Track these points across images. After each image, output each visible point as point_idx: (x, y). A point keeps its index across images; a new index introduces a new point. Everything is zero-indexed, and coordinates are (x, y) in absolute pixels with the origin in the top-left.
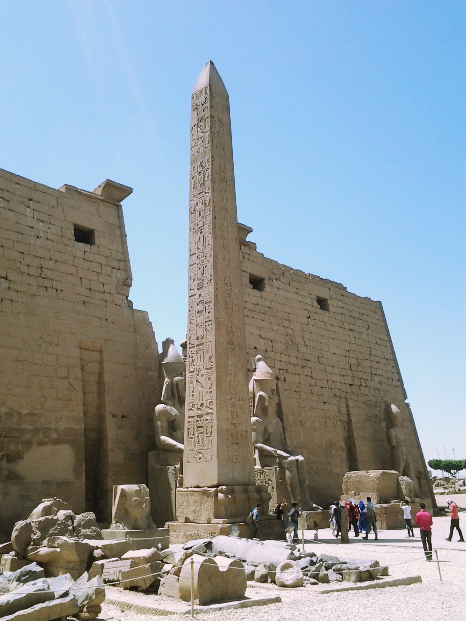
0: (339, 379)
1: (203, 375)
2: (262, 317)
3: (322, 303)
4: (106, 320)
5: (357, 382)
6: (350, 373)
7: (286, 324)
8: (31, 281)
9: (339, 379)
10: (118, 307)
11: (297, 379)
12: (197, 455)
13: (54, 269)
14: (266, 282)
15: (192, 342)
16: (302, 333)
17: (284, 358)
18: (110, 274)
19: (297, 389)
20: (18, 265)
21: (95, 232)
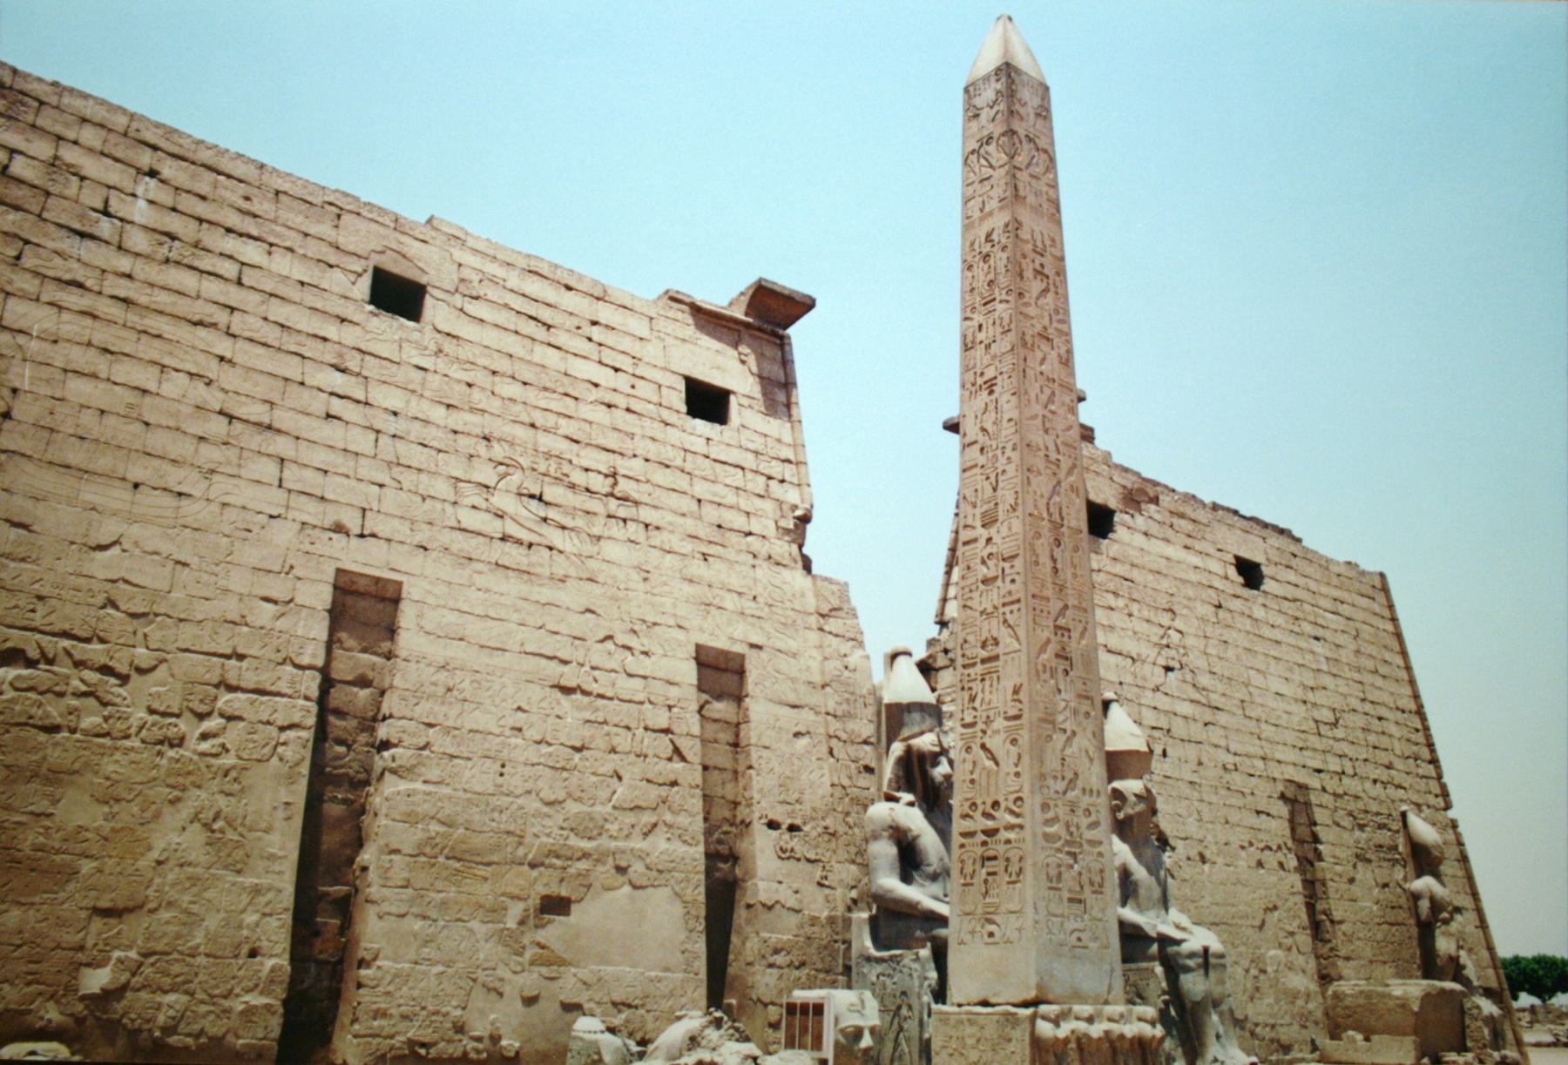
0: (1292, 755)
1: (997, 732)
3: (1250, 573)
4: (755, 598)
8: (594, 505)
9: (1292, 755)
10: (780, 569)
11: (1192, 752)
12: (982, 927)
13: (643, 479)
14: (1116, 518)
15: (968, 653)
16: (1203, 642)
17: (1162, 702)
18: (762, 493)
19: (1195, 778)
20: (566, 468)
21: (732, 398)
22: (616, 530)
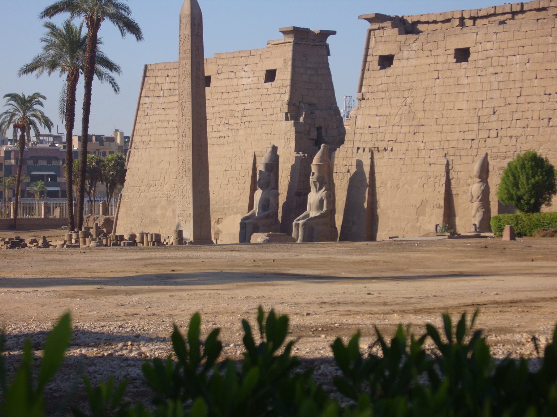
2: (383, 95)
5: (483, 134)
6: (476, 127)
7: (406, 94)
8: (239, 121)
9: (457, 136)
11: (404, 146)
17: (396, 129)
19: (403, 156)
22: (243, 126)
